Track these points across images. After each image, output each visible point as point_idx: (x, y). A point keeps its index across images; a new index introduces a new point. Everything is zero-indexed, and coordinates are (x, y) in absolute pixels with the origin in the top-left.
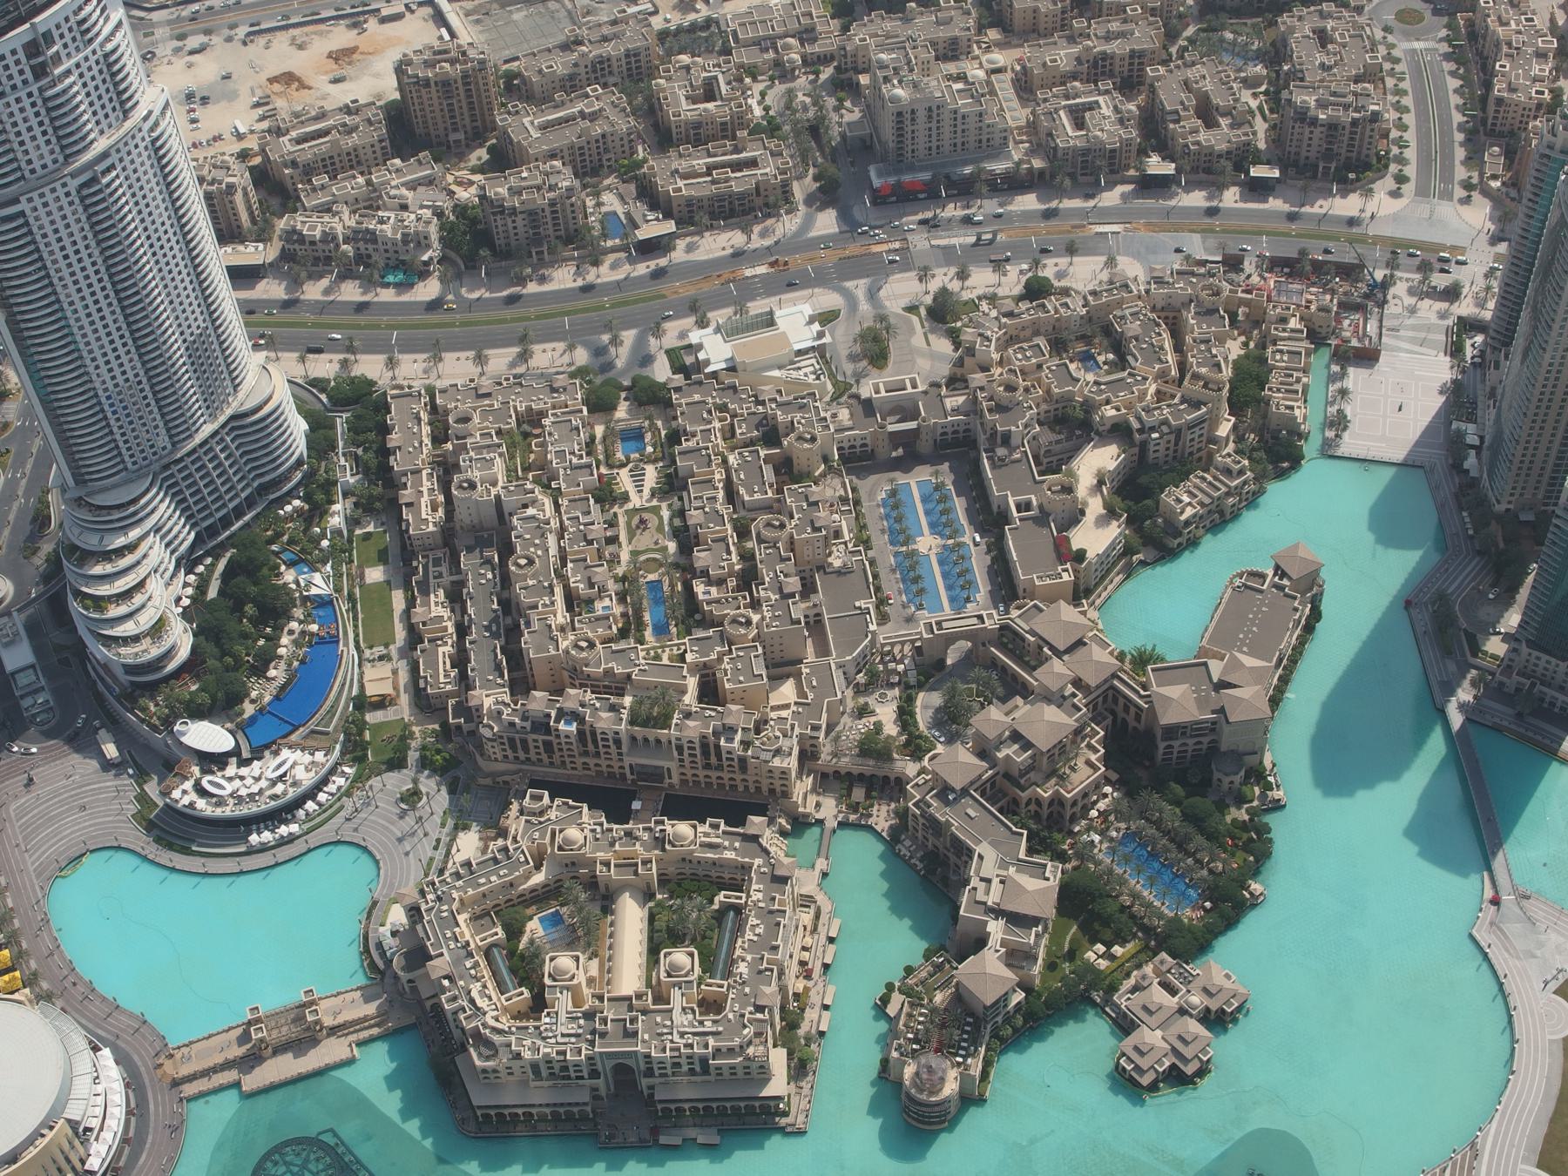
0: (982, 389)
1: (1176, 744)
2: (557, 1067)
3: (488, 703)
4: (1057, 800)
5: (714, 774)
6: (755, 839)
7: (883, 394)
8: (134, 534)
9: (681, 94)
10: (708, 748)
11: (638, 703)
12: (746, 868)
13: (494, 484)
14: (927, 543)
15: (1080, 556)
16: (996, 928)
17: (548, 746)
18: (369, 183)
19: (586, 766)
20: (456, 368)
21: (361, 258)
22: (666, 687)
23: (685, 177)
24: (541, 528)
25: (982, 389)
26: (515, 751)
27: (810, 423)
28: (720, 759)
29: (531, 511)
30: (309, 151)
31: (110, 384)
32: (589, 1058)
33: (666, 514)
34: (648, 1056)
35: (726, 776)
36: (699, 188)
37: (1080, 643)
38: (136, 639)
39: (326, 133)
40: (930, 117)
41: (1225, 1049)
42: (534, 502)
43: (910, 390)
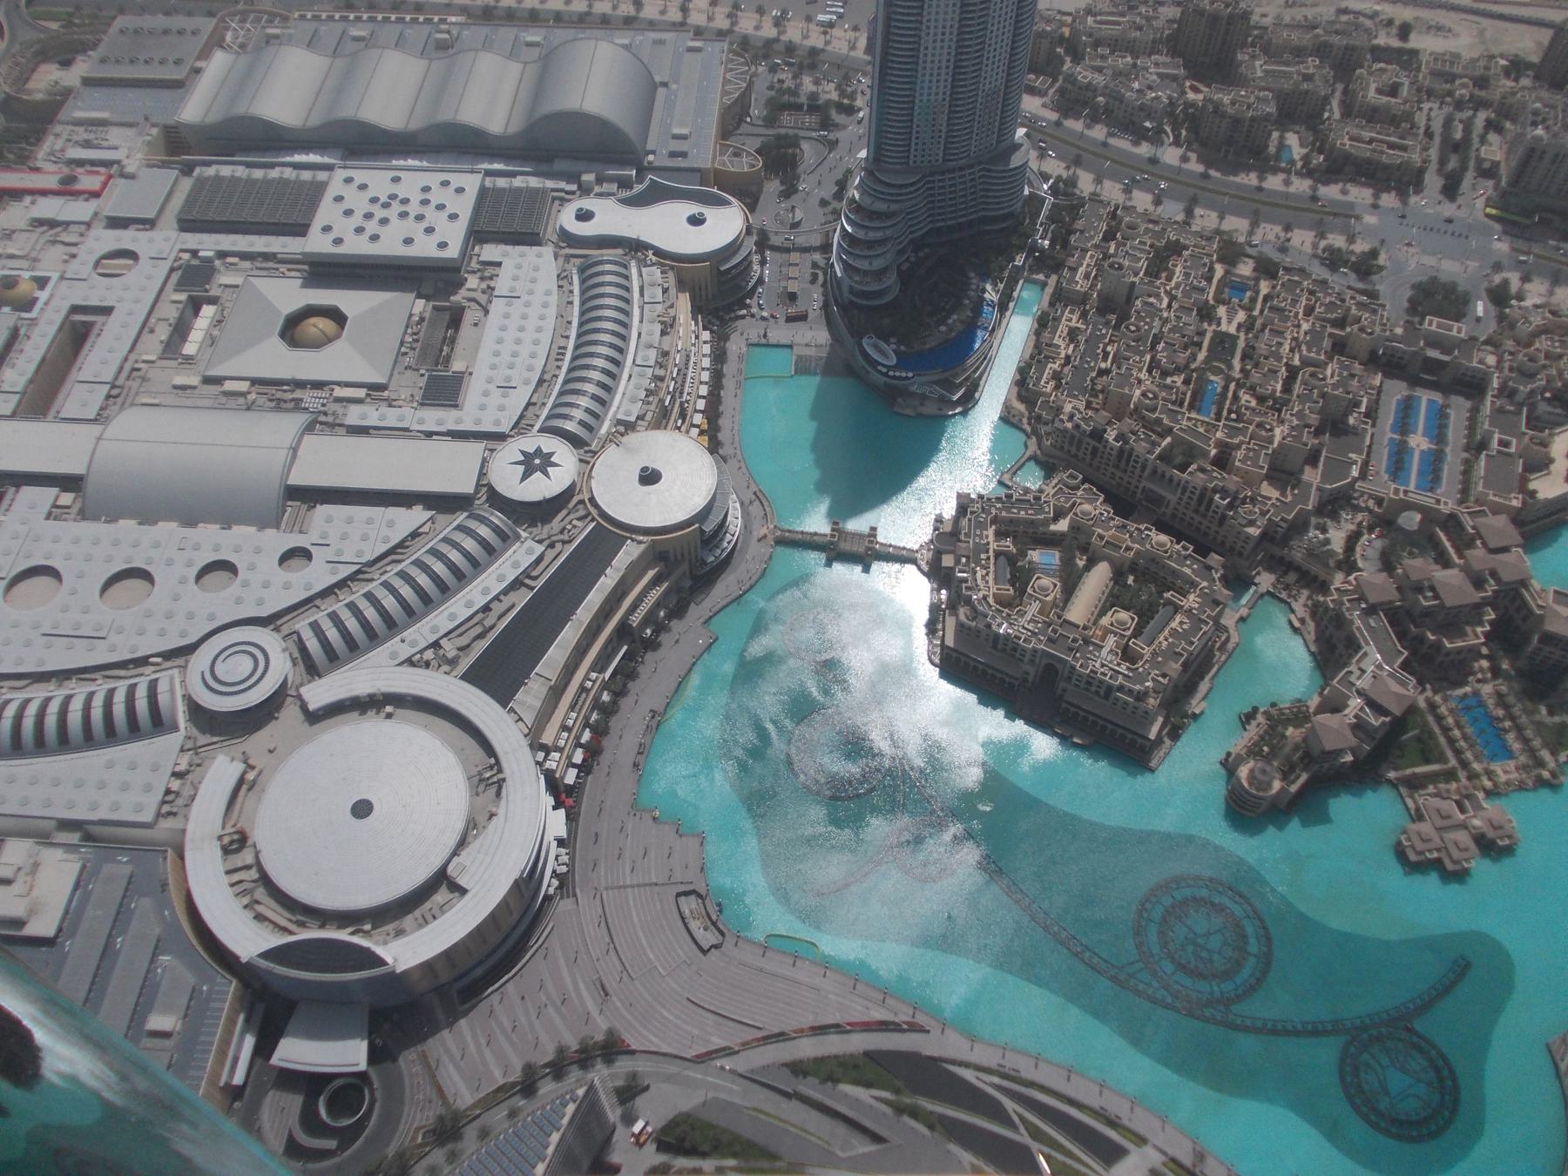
0: (1511, 353)
1: (1547, 649)
2: (1010, 645)
3: (1068, 408)
4: (1438, 647)
5: (1198, 518)
6: (1209, 568)
7: (1433, 328)
8: (894, 207)
9: (1373, 86)
10: (1204, 497)
11: (1171, 446)
12: (1194, 585)
13: (1136, 275)
14: (1419, 442)
15: (1533, 493)
16: (1355, 702)
17: (1095, 451)
18: (1135, 65)
19: (1113, 476)
20: (1142, 200)
21: (1108, 111)
22: (1192, 446)
23: (1351, 139)
24: (1154, 311)
25: (1511, 353)
26: (1071, 444)
27: (1373, 323)
28: (1207, 510)
29: (1152, 300)
30: (1108, 31)
31: (925, 98)
32: (1035, 650)
33: (1241, 344)
34: (1073, 668)
35: (1206, 523)
36: (1364, 151)
37: (1505, 550)
38: (866, 273)
39: (1118, 24)
40: (1553, 162)
41: (1481, 867)
42: (1157, 296)
43: (1454, 333)
